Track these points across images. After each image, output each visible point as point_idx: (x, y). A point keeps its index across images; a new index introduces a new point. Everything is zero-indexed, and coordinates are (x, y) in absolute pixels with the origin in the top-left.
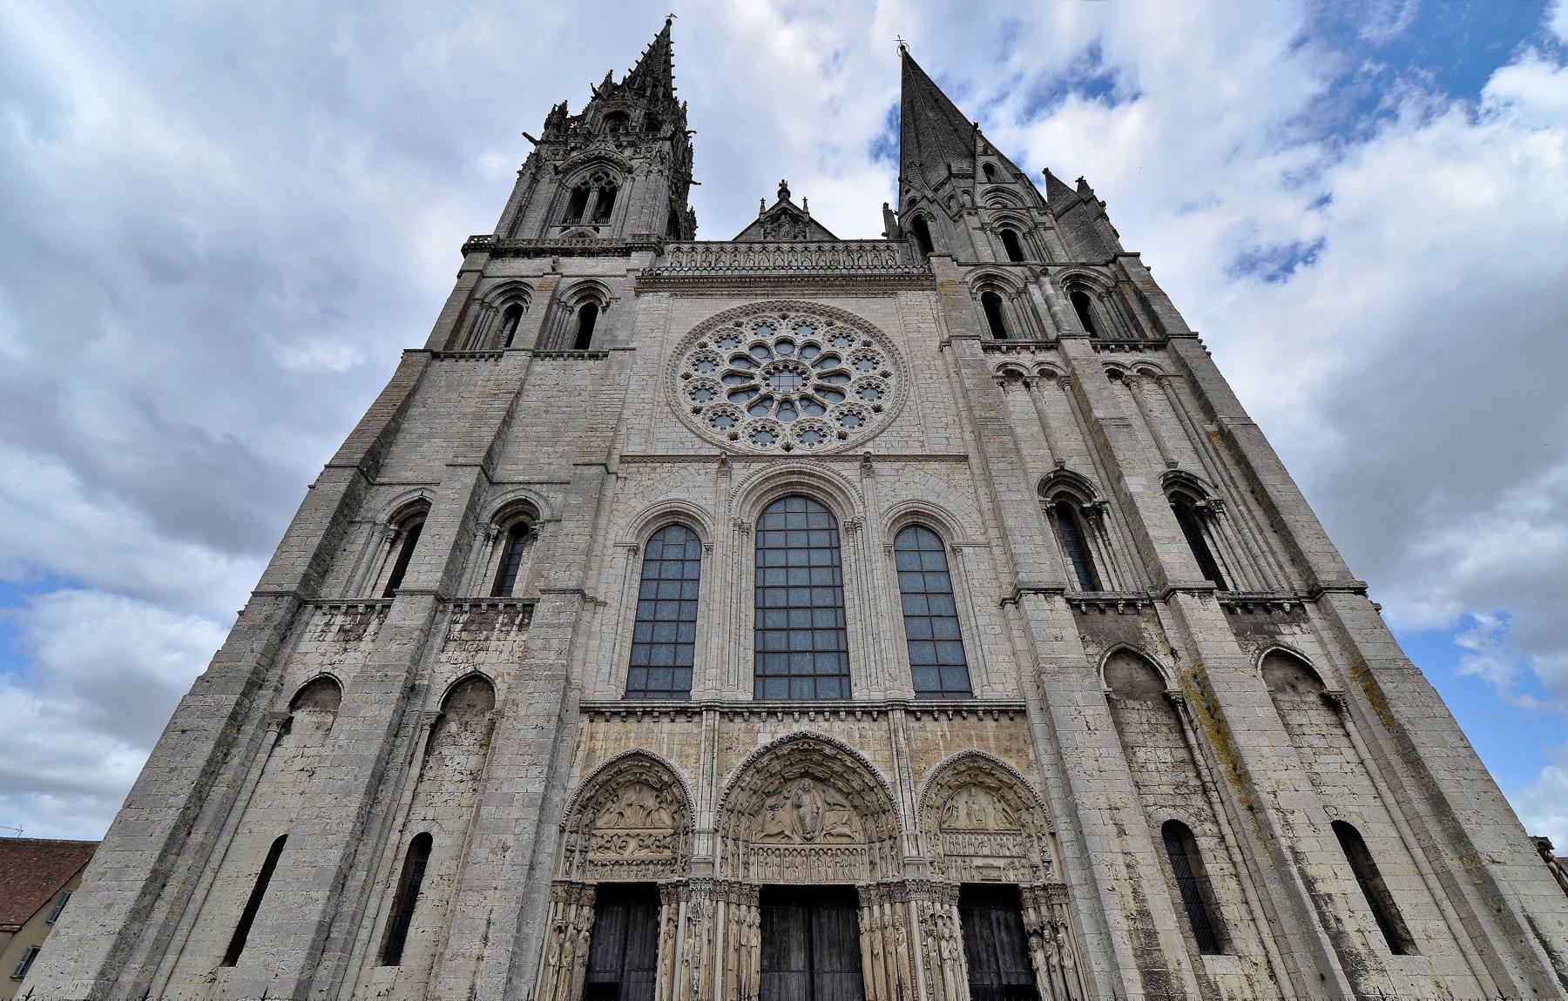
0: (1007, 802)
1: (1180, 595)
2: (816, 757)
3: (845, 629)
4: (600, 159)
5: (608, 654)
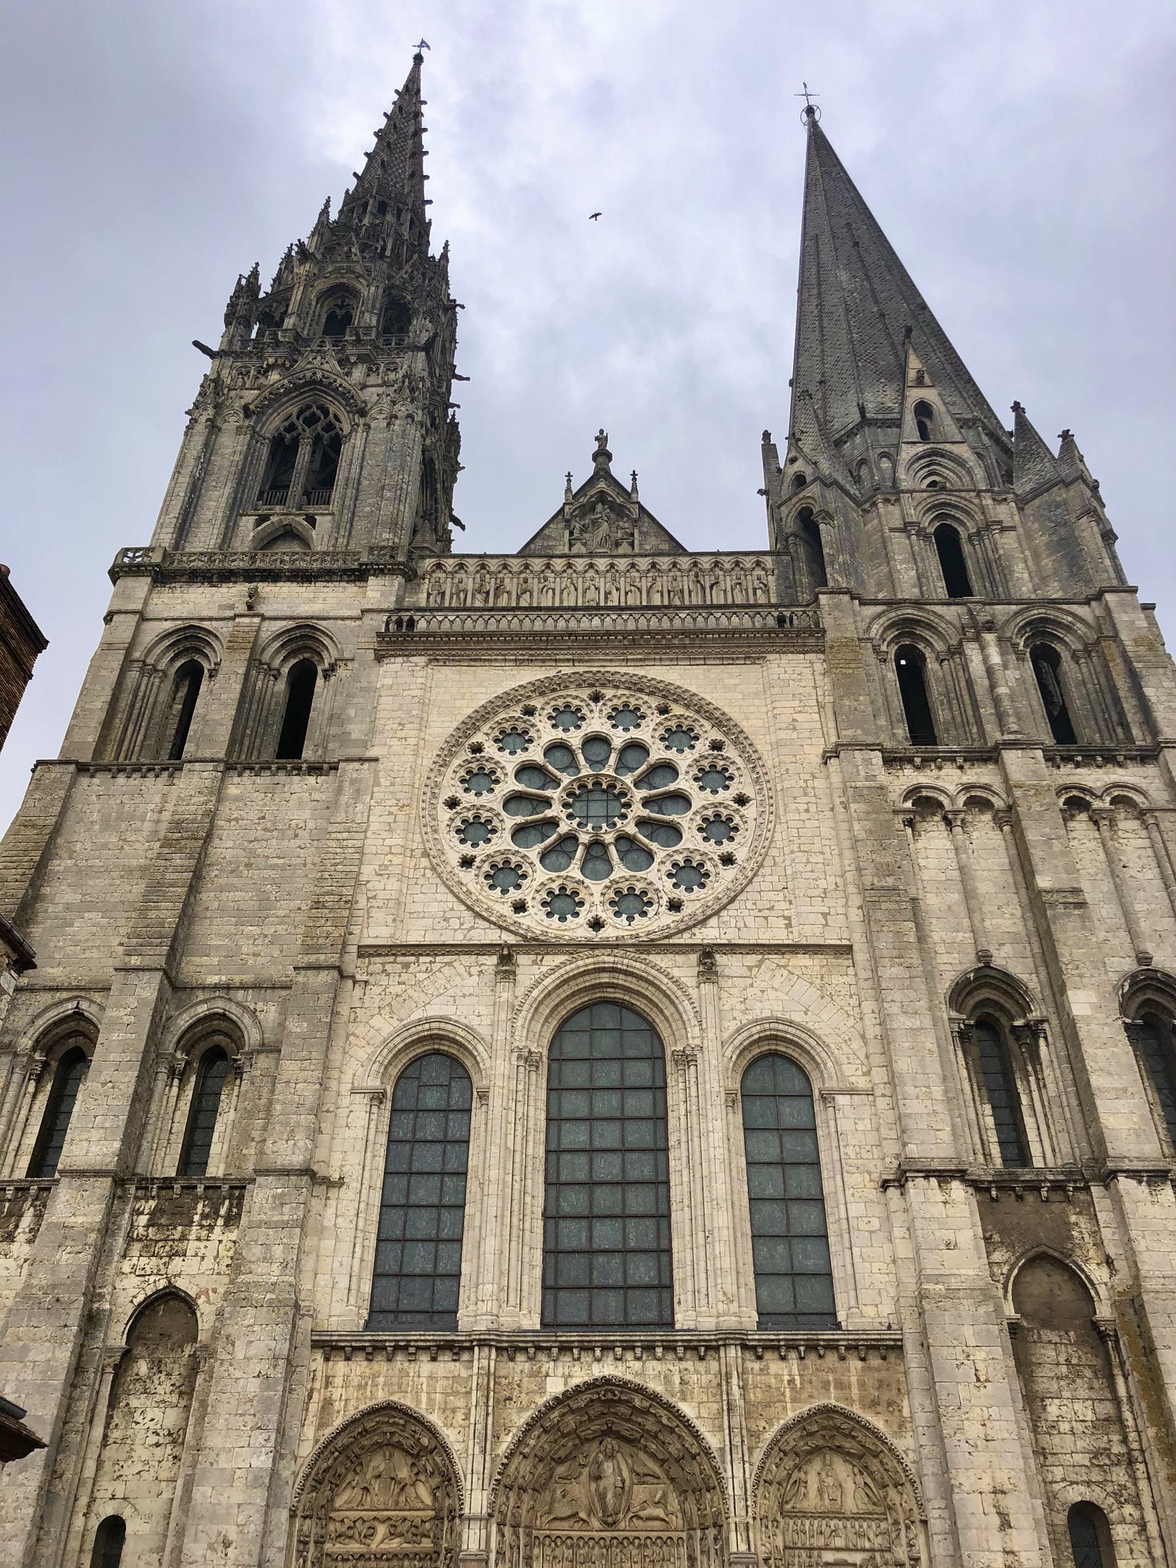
0: (871, 1474)
1: (1125, 1184)
2: (622, 1409)
3: (668, 1216)
4: (314, 385)
5: (347, 1261)
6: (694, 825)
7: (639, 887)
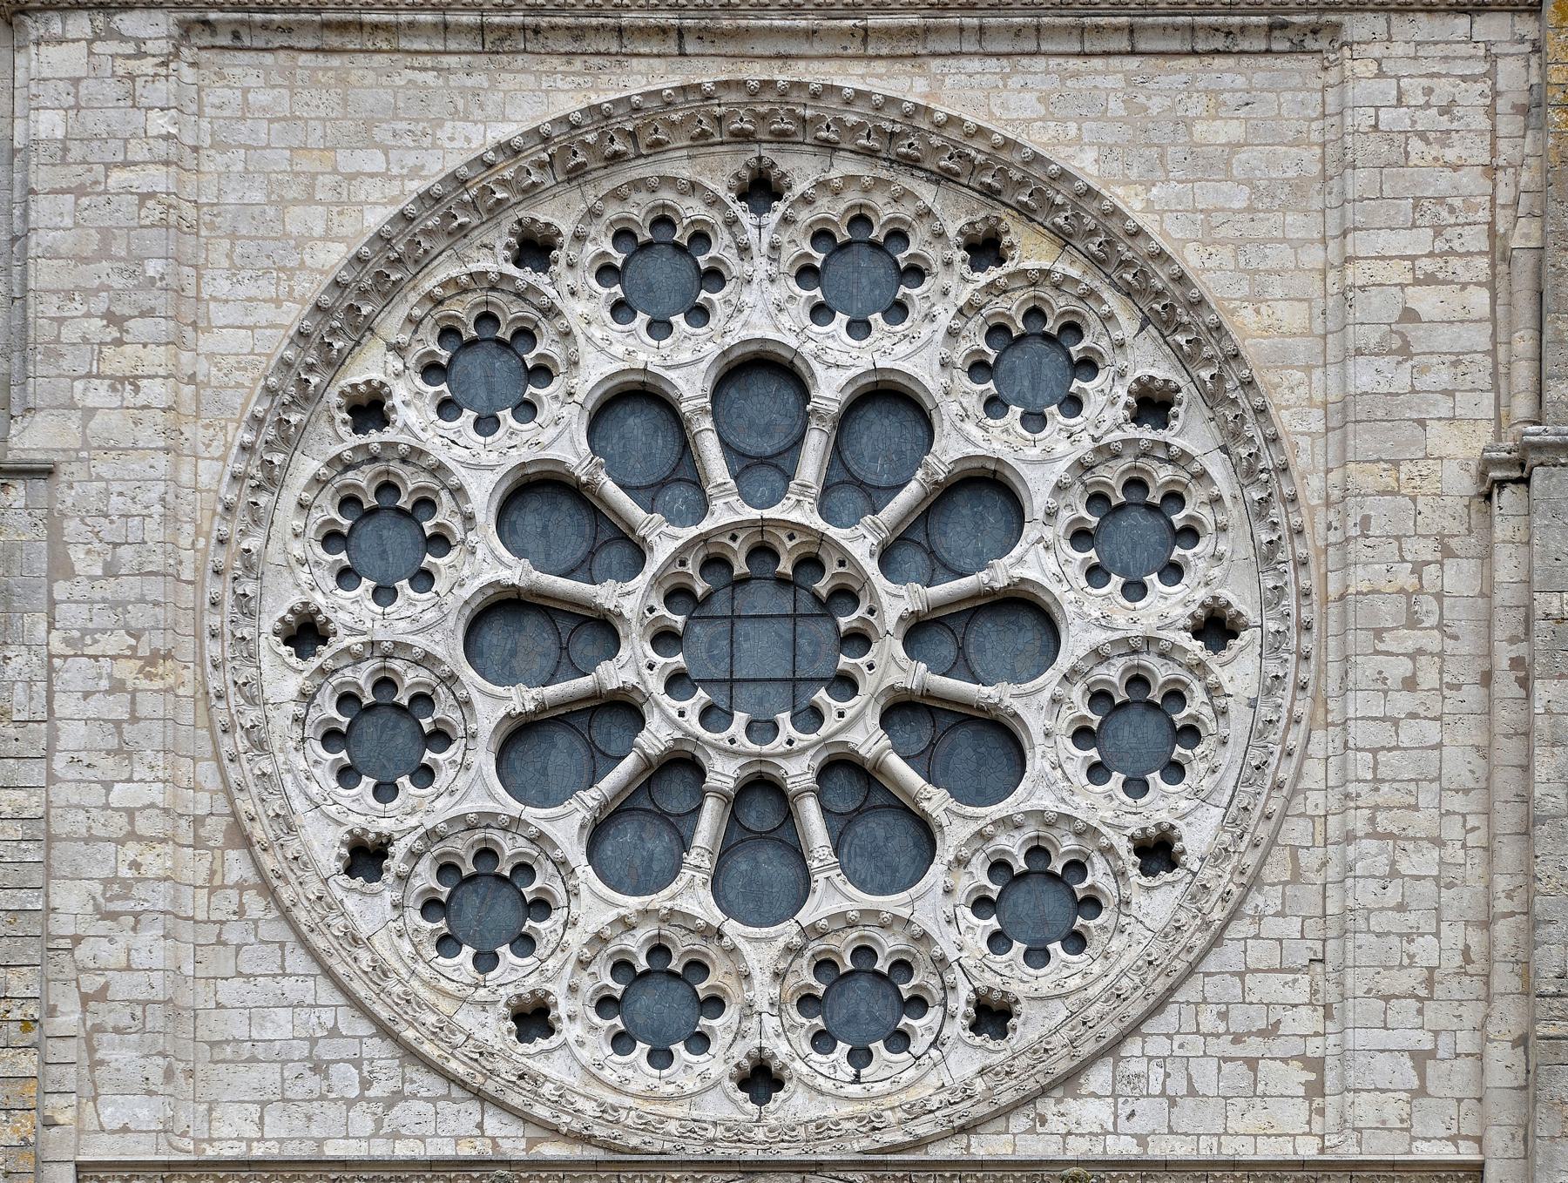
6: (1064, 725)
7: (889, 945)
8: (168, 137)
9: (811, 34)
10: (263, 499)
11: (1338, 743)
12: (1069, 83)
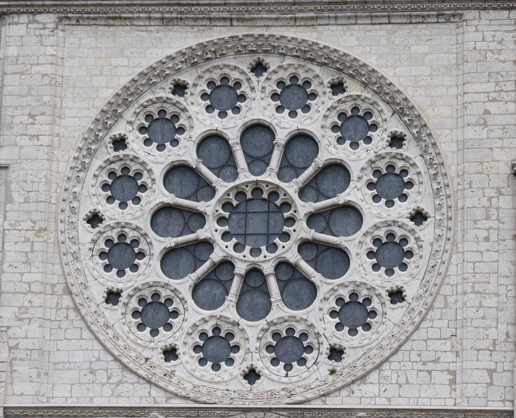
7: (299, 328)
8: (53, 55)
9: (277, 19)
10: (81, 174)
11: (461, 259)
12: (367, 33)
